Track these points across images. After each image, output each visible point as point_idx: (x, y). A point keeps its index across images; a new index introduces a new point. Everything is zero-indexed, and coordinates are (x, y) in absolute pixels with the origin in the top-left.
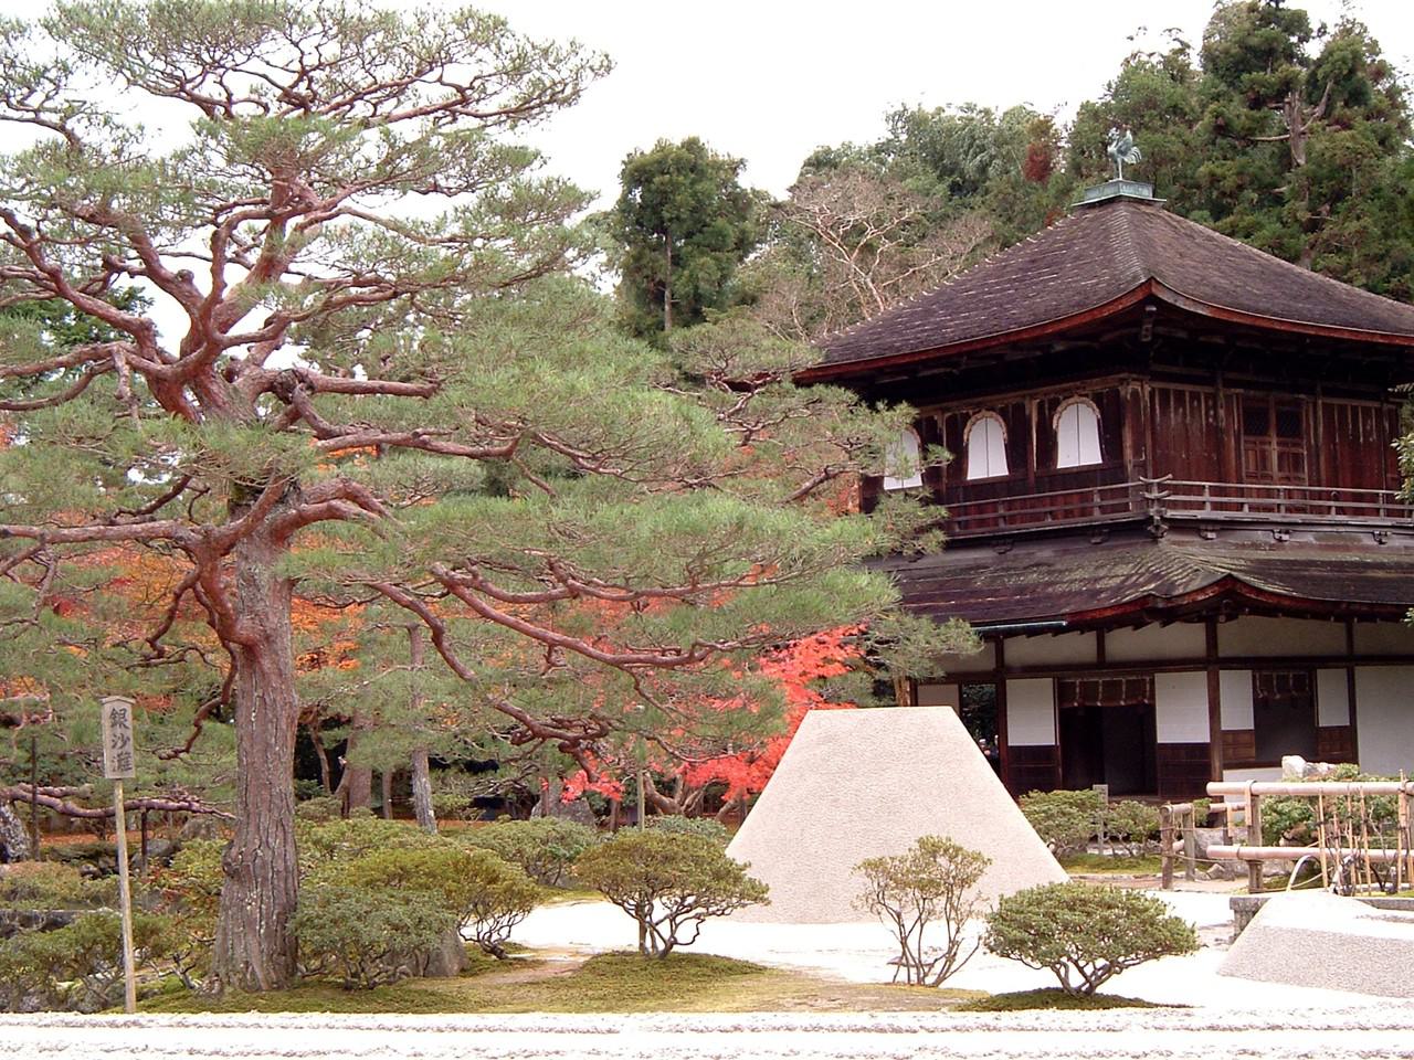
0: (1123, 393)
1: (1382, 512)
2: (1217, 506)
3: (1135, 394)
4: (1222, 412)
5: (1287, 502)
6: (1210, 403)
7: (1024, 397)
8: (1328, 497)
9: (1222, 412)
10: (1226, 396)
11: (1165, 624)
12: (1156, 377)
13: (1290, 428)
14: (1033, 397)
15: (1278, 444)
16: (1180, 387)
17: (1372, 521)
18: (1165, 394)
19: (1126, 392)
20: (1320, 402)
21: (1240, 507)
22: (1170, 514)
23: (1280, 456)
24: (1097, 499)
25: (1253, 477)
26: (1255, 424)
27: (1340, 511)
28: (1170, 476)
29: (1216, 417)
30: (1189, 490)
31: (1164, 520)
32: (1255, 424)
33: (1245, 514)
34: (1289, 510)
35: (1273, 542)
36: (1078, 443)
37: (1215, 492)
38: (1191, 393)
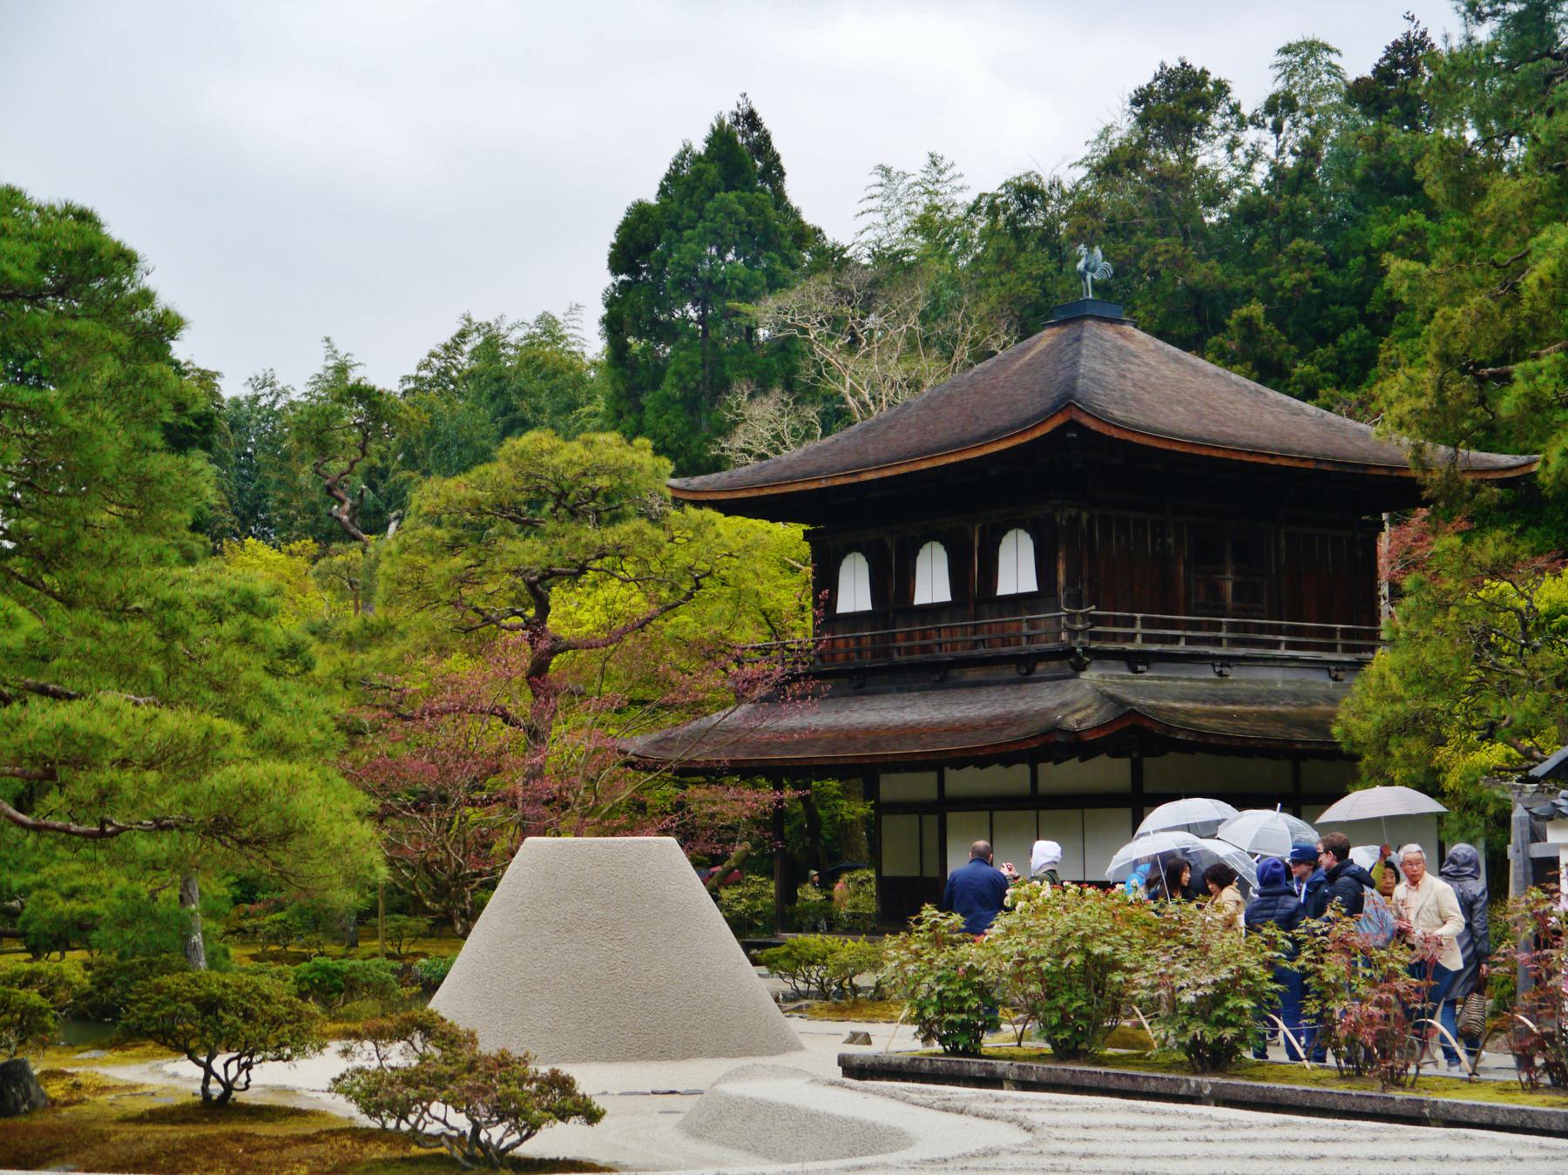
2: (1147, 639)
4: (1170, 541)
5: (1231, 635)
8: (1278, 630)
9: (1170, 541)
11: (1082, 760)
15: (1235, 573)
19: (1061, 519)
21: (1175, 640)
24: (1025, 629)
27: (1290, 646)
30: (1116, 622)
31: (1086, 651)
33: (1181, 648)
35: (1214, 676)
36: (1017, 570)
37: (1147, 623)
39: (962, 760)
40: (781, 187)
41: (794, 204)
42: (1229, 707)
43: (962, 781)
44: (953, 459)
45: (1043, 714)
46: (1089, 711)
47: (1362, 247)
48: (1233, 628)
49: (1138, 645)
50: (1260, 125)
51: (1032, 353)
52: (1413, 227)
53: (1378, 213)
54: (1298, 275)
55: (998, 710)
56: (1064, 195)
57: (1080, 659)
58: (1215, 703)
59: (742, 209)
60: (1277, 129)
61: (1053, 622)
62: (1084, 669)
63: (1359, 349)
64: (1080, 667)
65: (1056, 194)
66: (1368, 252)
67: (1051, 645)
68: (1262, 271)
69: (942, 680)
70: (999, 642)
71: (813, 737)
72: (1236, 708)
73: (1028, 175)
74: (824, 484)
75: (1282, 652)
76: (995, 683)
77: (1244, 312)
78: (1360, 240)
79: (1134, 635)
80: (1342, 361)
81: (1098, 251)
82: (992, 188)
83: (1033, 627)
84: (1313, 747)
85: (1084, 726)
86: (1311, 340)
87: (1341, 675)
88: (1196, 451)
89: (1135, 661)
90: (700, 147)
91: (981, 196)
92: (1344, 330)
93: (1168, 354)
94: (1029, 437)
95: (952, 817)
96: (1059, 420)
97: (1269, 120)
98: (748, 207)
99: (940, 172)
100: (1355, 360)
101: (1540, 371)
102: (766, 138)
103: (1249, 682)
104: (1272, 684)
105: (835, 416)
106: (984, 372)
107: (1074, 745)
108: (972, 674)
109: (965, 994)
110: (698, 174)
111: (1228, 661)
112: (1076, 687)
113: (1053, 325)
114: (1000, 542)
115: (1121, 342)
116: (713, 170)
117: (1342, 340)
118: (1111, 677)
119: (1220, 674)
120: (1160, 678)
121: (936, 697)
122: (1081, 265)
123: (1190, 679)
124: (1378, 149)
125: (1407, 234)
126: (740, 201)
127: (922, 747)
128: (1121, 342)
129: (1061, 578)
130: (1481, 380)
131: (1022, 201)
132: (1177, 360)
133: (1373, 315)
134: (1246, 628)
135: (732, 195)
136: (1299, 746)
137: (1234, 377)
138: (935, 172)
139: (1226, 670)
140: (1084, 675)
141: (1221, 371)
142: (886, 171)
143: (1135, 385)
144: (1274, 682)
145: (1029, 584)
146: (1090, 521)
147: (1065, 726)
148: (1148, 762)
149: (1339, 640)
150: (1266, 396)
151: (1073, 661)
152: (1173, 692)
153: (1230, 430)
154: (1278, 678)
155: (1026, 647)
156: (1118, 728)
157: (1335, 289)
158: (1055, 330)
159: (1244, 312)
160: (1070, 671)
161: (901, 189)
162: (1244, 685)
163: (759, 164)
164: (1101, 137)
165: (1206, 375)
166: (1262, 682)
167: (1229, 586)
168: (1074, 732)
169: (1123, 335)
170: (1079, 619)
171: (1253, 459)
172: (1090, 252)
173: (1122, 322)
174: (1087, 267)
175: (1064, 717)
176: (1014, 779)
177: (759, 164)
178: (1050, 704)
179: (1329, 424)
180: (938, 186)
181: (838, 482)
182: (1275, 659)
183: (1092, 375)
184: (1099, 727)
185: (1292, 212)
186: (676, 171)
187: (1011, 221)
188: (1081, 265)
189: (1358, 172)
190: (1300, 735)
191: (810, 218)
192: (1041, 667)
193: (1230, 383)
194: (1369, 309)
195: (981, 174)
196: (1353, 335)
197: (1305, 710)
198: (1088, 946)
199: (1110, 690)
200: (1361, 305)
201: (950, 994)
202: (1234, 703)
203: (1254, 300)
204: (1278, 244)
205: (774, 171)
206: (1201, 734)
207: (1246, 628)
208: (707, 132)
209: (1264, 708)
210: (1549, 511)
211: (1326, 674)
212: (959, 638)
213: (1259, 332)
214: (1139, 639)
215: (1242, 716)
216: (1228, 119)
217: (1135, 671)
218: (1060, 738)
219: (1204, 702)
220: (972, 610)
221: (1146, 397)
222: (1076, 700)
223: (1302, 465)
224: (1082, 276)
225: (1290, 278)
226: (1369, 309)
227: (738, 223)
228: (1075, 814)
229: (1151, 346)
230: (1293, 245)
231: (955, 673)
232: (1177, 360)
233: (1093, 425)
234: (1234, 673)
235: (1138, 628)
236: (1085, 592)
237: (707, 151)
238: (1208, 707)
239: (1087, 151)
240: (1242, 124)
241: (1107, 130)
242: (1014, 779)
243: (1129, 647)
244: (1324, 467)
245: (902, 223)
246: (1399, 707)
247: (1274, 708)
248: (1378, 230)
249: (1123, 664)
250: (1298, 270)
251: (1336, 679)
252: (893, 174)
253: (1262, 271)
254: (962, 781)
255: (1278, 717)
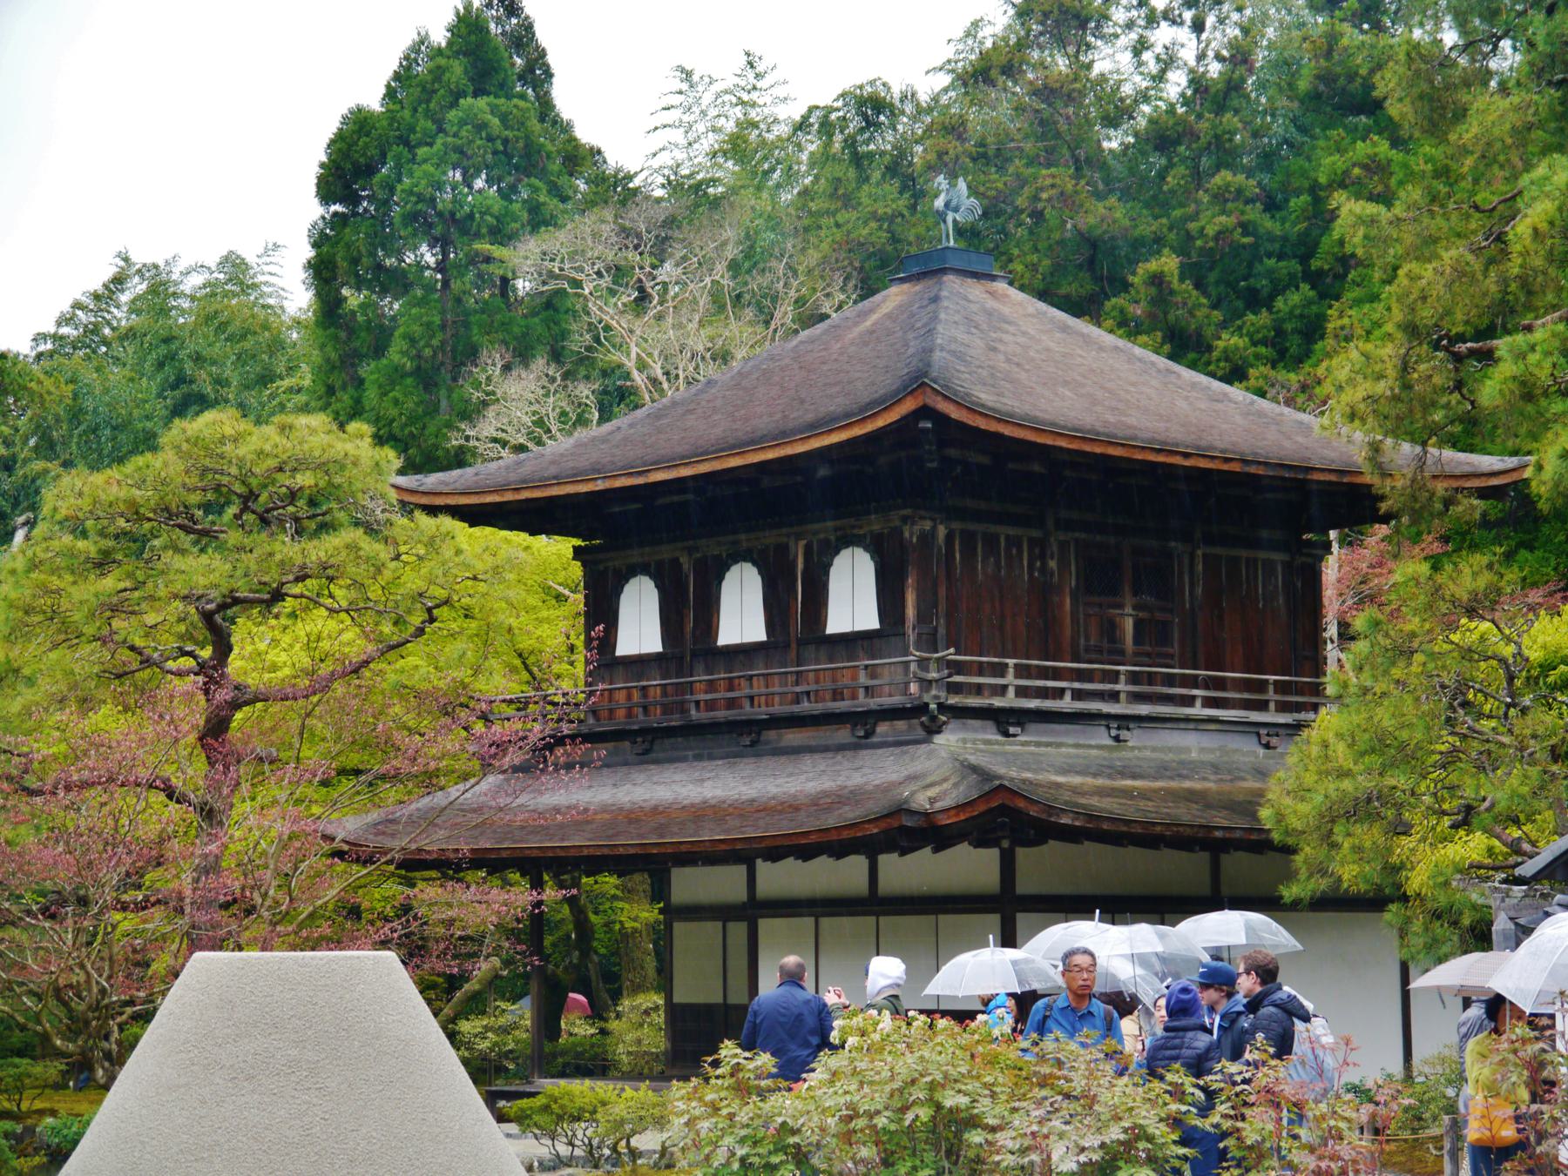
0: (907, 535)
1: (1272, 706)
2: (1022, 692)
3: (927, 539)
4: (1053, 564)
6: (1037, 551)
7: (788, 536)
8: (1193, 682)
9: (1053, 564)
10: (1063, 546)
11: (936, 850)
12: (951, 514)
13: (1156, 581)
14: (798, 537)
16: (993, 528)
17: (1255, 716)
18: (969, 540)
19: (911, 533)
20: (1199, 552)
21: (1059, 693)
22: (953, 700)
23: (1138, 624)
24: (863, 679)
25: (1096, 654)
26: (1100, 580)
28: (952, 650)
29: (1044, 569)
30: (981, 669)
31: (942, 707)
32: (1100, 580)
33: (1067, 704)
34: (1137, 698)
35: (1110, 742)
36: (852, 600)
37: (1022, 672)
38: (1008, 537)
39: (776, 851)
40: (547, 93)
41: (565, 116)
42: (1129, 783)
43: (777, 878)
44: (770, 455)
45: (886, 789)
46: (945, 786)
47: (1306, 184)
48: (1134, 678)
49: (1010, 700)
50: (1176, 22)
51: (875, 317)
52: (1373, 158)
53: (1327, 138)
54: (1223, 218)
55: (827, 784)
56: (920, 111)
57: (934, 718)
58: (1110, 777)
59: (496, 121)
60: (1198, 27)
61: (900, 669)
62: (939, 732)
63: (1301, 316)
64: (933, 729)
65: (909, 108)
66: (1314, 189)
67: (896, 700)
68: (1177, 213)
69: (753, 744)
70: (828, 696)
71: (583, 818)
72: (1138, 783)
73: (872, 83)
74: (601, 485)
75: (1198, 710)
76: (824, 749)
77: (1153, 266)
78: (1304, 174)
79: (1005, 687)
80: (1280, 332)
81: (962, 185)
82: (826, 97)
83: (873, 676)
84: (1238, 834)
85: (939, 805)
86: (1240, 304)
87: (1274, 741)
88: (1087, 448)
89: (1005, 720)
90: (440, 37)
91: (812, 109)
92: (1282, 292)
93: (1052, 320)
94: (869, 427)
95: (764, 925)
96: (908, 406)
97: (1188, 15)
98: (504, 118)
99: (758, 76)
100: (1295, 331)
101: (1533, 348)
102: (528, 27)
103: (1154, 749)
104: (1180, 755)
105: (616, 397)
106: (811, 341)
107: (929, 833)
108: (793, 737)
109: (775, 1159)
110: (438, 73)
111: (1125, 721)
112: (930, 754)
113: (903, 280)
114: (830, 565)
115: (991, 303)
116: (457, 70)
117: (1279, 303)
118: (974, 742)
119: (1117, 739)
120: (1038, 744)
121: (747, 766)
122: (939, 203)
123: (1077, 746)
124: (1328, 54)
125: (1365, 167)
126: (494, 110)
127: (727, 831)
128: (991, 303)
129: (910, 612)
130: (1458, 358)
131: (865, 117)
132: (1065, 328)
133: (1320, 273)
134: (1151, 679)
135: (482, 102)
136: (1218, 834)
137: (1138, 351)
138: (751, 75)
139: (1124, 734)
140: (939, 739)
141: (1121, 343)
142: (688, 75)
143: (1008, 361)
144: (1188, 750)
145: (868, 619)
146: (950, 538)
147: (914, 806)
148: (1022, 853)
149: (1271, 695)
150: (1179, 376)
151: (924, 720)
152: (1057, 764)
153: (1132, 421)
154: (1192, 745)
155: (863, 702)
156: (982, 808)
157: (1272, 239)
158: (906, 286)
159: (1153, 266)
160: (921, 733)
161: (707, 98)
162: (1148, 753)
163: (519, 61)
164: (968, 34)
165: (1101, 349)
166: (1170, 749)
167: (1129, 624)
168: (926, 815)
169: (992, 293)
170: (933, 666)
171: (1161, 458)
172: (952, 185)
173: (993, 278)
174: (947, 205)
175: (913, 794)
176: (849, 874)
177: (519, 61)
178: (894, 777)
179: (1261, 414)
180: (754, 95)
181: (619, 483)
182: (1187, 720)
183: (953, 347)
184: (959, 808)
185: (1216, 136)
186: (409, 68)
187: (850, 143)
188: (939, 203)
189: (1303, 85)
190: (1220, 819)
191: (586, 134)
192: (882, 728)
193: (1131, 359)
194: (1315, 264)
195: (808, 83)
196: (1295, 298)
197: (1226, 787)
198: (938, 1096)
199: (973, 759)
200: (1305, 259)
201: (756, 1160)
202: (1134, 777)
203: (1166, 251)
204: (1198, 177)
205: (538, 72)
206: (1091, 817)
207: (1151, 679)
208: (450, 18)
209: (1173, 784)
210: (1546, 529)
211: (1255, 739)
212: (777, 689)
213: (1172, 292)
214: (1011, 692)
215: (1144, 795)
216: (1134, 13)
217: (1006, 734)
218: (908, 822)
219: (1095, 775)
220: (793, 654)
221: (1023, 376)
222: (931, 771)
223: (1225, 467)
224: (941, 216)
225: (1213, 222)
226: (1315, 264)
227: (490, 139)
228: (924, 921)
229: (1031, 310)
230: (1217, 180)
231: (771, 735)
232: (1065, 328)
233: (955, 413)
234: (1134, 738)
235: (1010, 679)
236: (942, 631)
237: (450, 43)
238: (1100, 782)
239: (949, 52)
240: (1152, 20)
241: (976, 24)
242: (849, 874)
243: (998, 702)
244: (1253, 469)
245: (709, 142)
246: (1347, 784)
247: (1187, 784)
248: (1329, 160)
249: (990, 724)
250: (1223, 212)
251: (1267, 746)
252: (696, 78)
253: (1177, 213)
254: (777, 878)
255: (1191, 796)
